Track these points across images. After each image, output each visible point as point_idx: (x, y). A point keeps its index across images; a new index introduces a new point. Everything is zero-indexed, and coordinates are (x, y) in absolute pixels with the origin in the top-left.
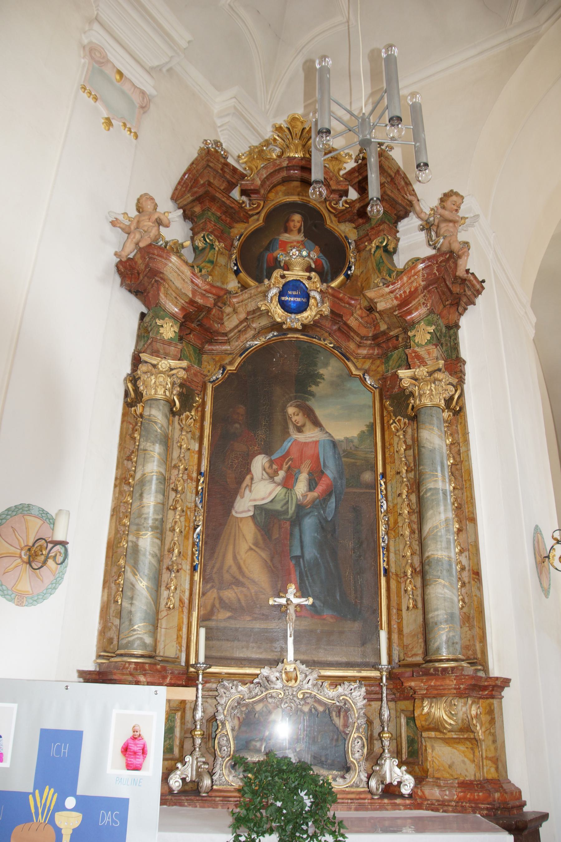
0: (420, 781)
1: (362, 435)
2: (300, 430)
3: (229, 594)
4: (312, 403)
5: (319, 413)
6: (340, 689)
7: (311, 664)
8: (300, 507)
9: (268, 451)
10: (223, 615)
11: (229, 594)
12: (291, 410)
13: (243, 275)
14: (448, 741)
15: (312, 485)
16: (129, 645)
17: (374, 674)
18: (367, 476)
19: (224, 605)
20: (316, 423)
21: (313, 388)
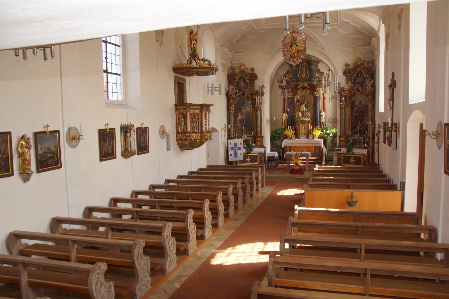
0: (256, 145)
1: (250, 110)
2: (243, 110)
3: (237, 129)
4: (245, 107)
5: (246, 108)
6: (249, 138)
7: (246, 135)
8: (244, 119)
9: (240, 113)
10: (237, 131)
11: (237, 129)
12: (242, 107)
13: (236, 89)
14: (259, 142)
15: (245, 117)
16: (232, 135)
17: (251, 136)
18: (250, 115)
19: (237, 130)
20: (245, 109)
21: (245, 105)
